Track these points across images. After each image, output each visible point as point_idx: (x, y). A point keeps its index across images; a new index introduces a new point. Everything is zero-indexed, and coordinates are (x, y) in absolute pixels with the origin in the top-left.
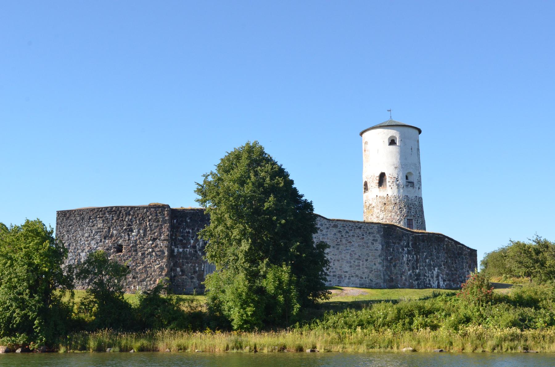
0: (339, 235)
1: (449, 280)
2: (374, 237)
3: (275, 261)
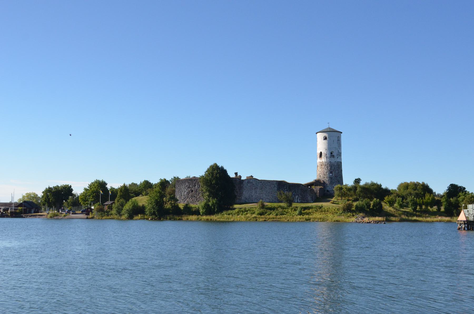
3: (213, 198)
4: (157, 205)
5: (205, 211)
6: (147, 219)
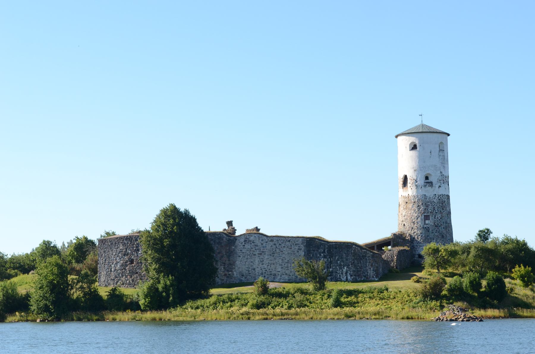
0: (274, 246)
1: (355, 275)
2: (299, 247)
3: (167, 275)
4: (52, 291)
5: (150, 302)
6: (34, 321)
